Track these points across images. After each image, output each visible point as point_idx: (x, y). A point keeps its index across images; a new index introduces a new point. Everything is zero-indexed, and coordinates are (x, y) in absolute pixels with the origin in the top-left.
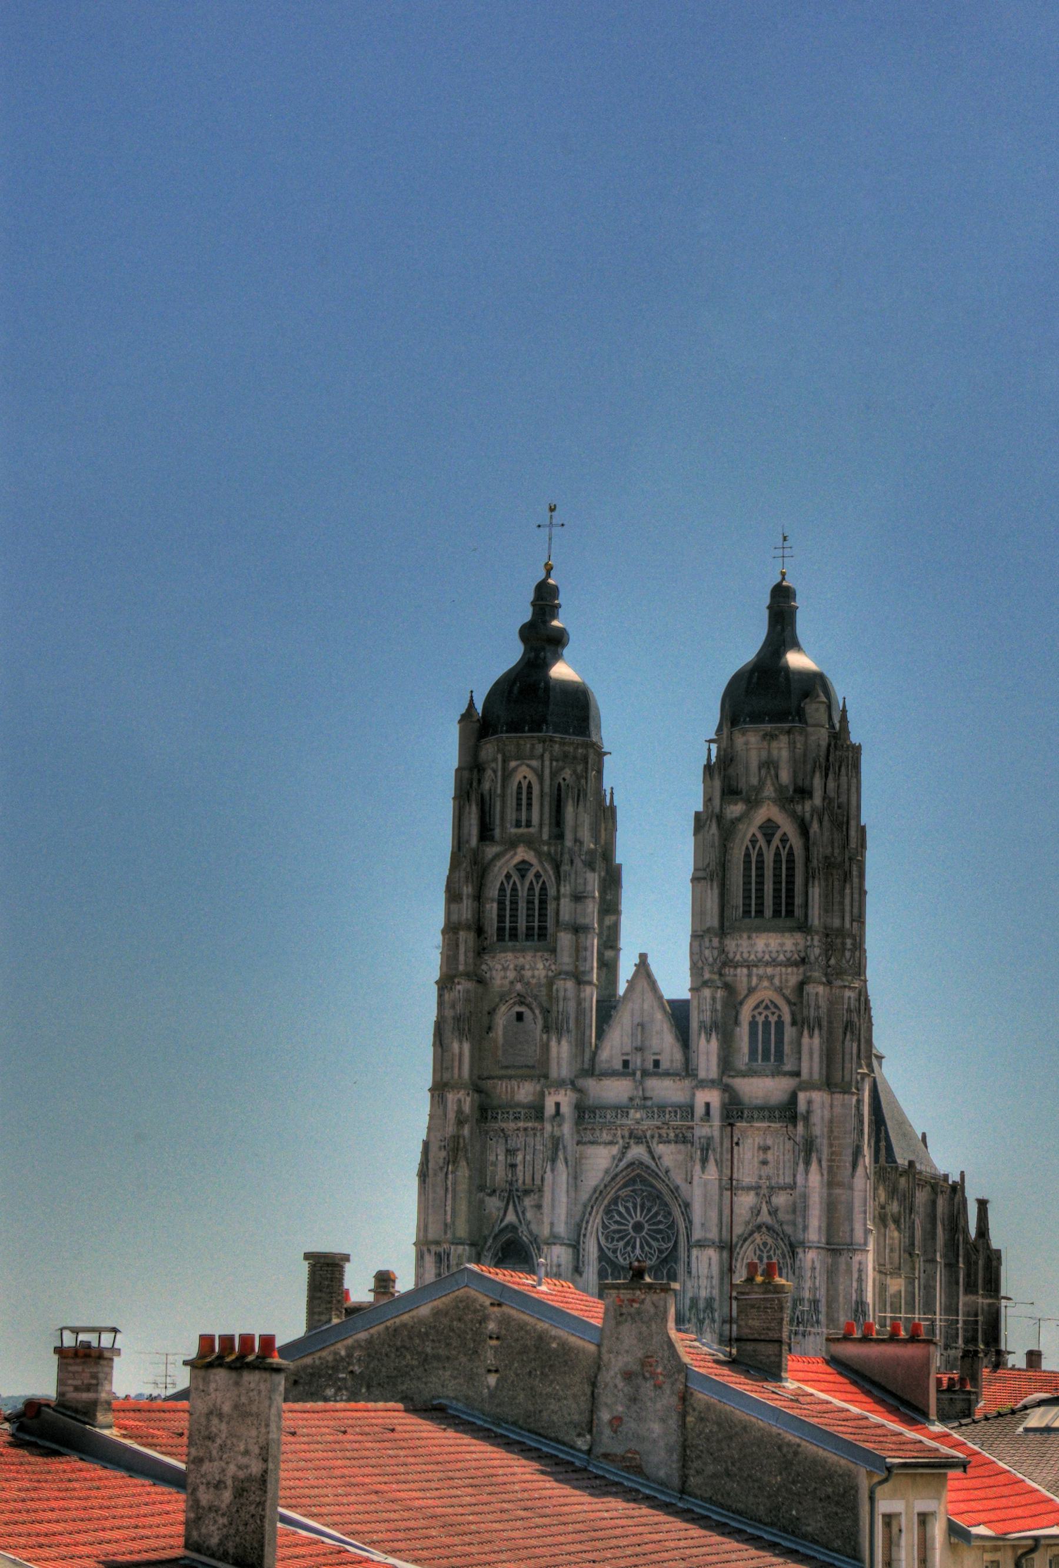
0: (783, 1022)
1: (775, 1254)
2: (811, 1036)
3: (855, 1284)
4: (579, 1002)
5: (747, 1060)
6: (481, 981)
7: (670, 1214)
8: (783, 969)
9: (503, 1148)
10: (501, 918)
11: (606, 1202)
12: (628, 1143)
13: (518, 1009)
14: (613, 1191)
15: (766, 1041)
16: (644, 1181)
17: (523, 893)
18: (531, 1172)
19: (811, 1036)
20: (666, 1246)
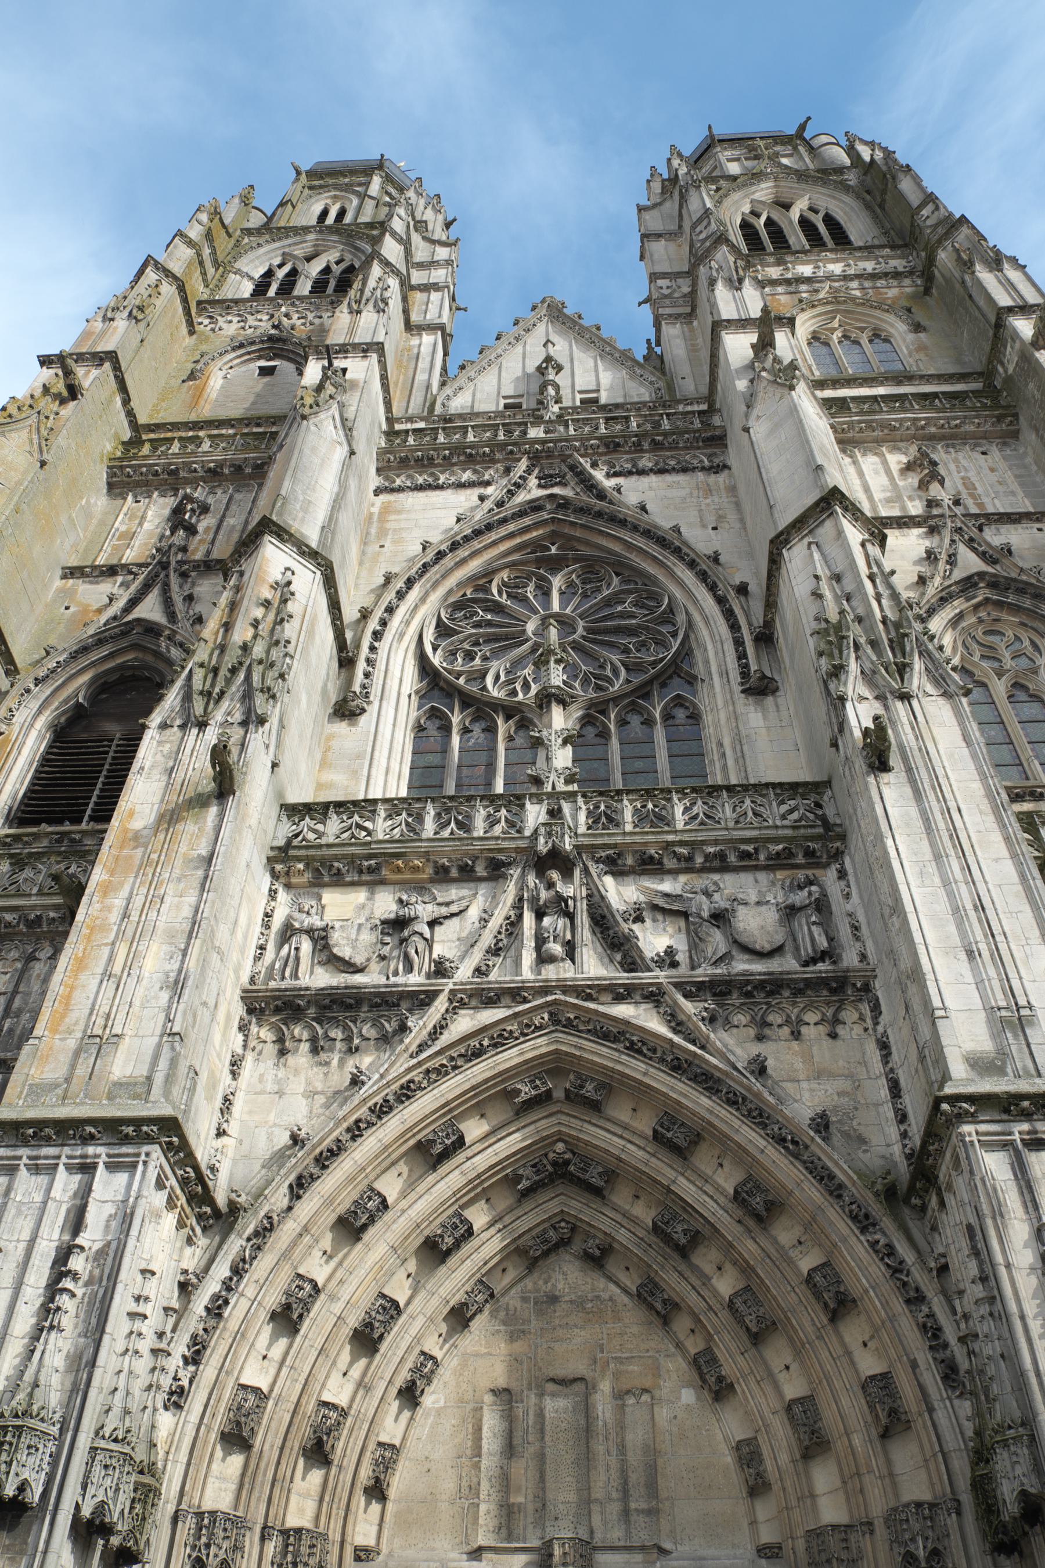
11: (451, 581)
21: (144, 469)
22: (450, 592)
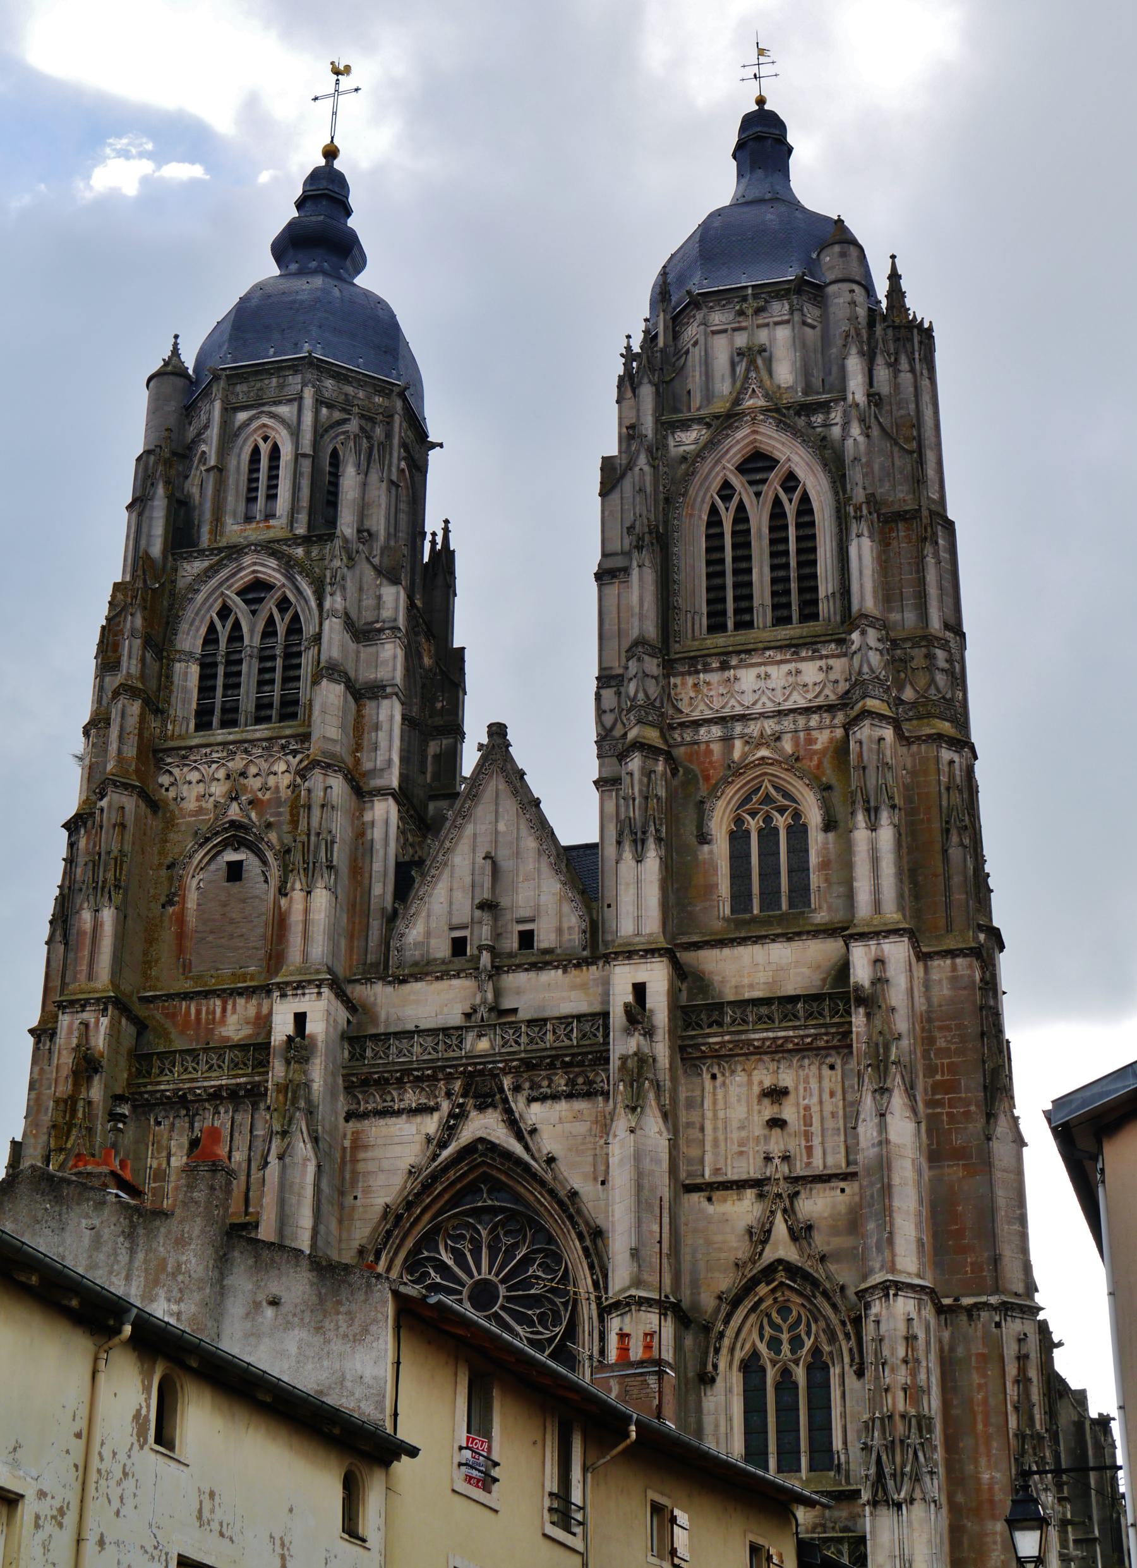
0: (805, 827)
1: (808, 1334)
2: (873, 828)
3: (1012, 1391)
4: (361, 833)
5: (728, 911)
6: (154, 804)
7: (558, 1258)
8: (801, 721)
9: (185, 1141)
10: (206, 689)
11: (410, 1243)
12: (460, 1106)
13: (231, 856)
14: (427, 1217)
15: (769, 873)
16: (497, 1187)
17: (252, 638)
18: (243, 1187)
19: (873, 828)
20: (548, 1335)
21: (158, 1095)
22: (406, 1260)
